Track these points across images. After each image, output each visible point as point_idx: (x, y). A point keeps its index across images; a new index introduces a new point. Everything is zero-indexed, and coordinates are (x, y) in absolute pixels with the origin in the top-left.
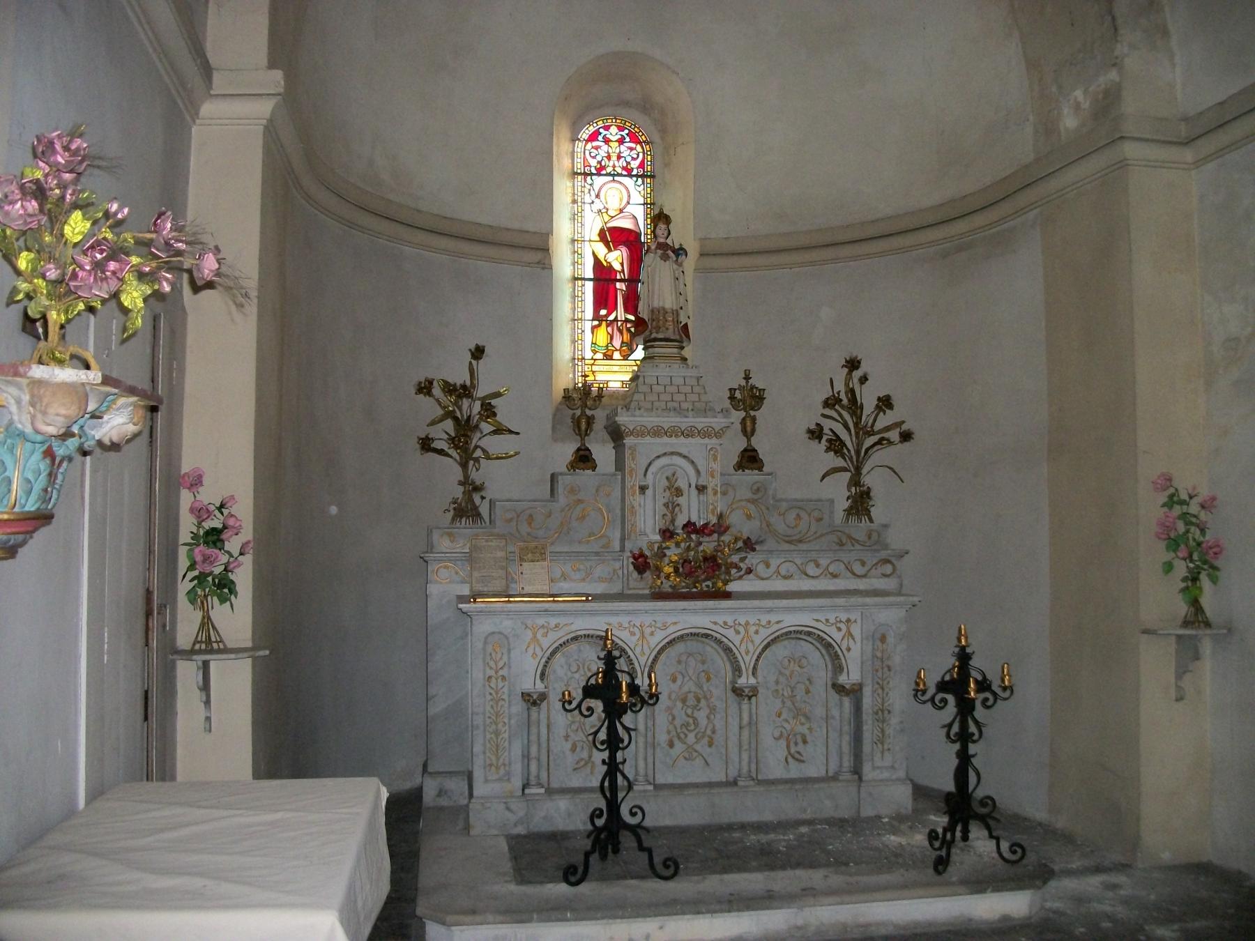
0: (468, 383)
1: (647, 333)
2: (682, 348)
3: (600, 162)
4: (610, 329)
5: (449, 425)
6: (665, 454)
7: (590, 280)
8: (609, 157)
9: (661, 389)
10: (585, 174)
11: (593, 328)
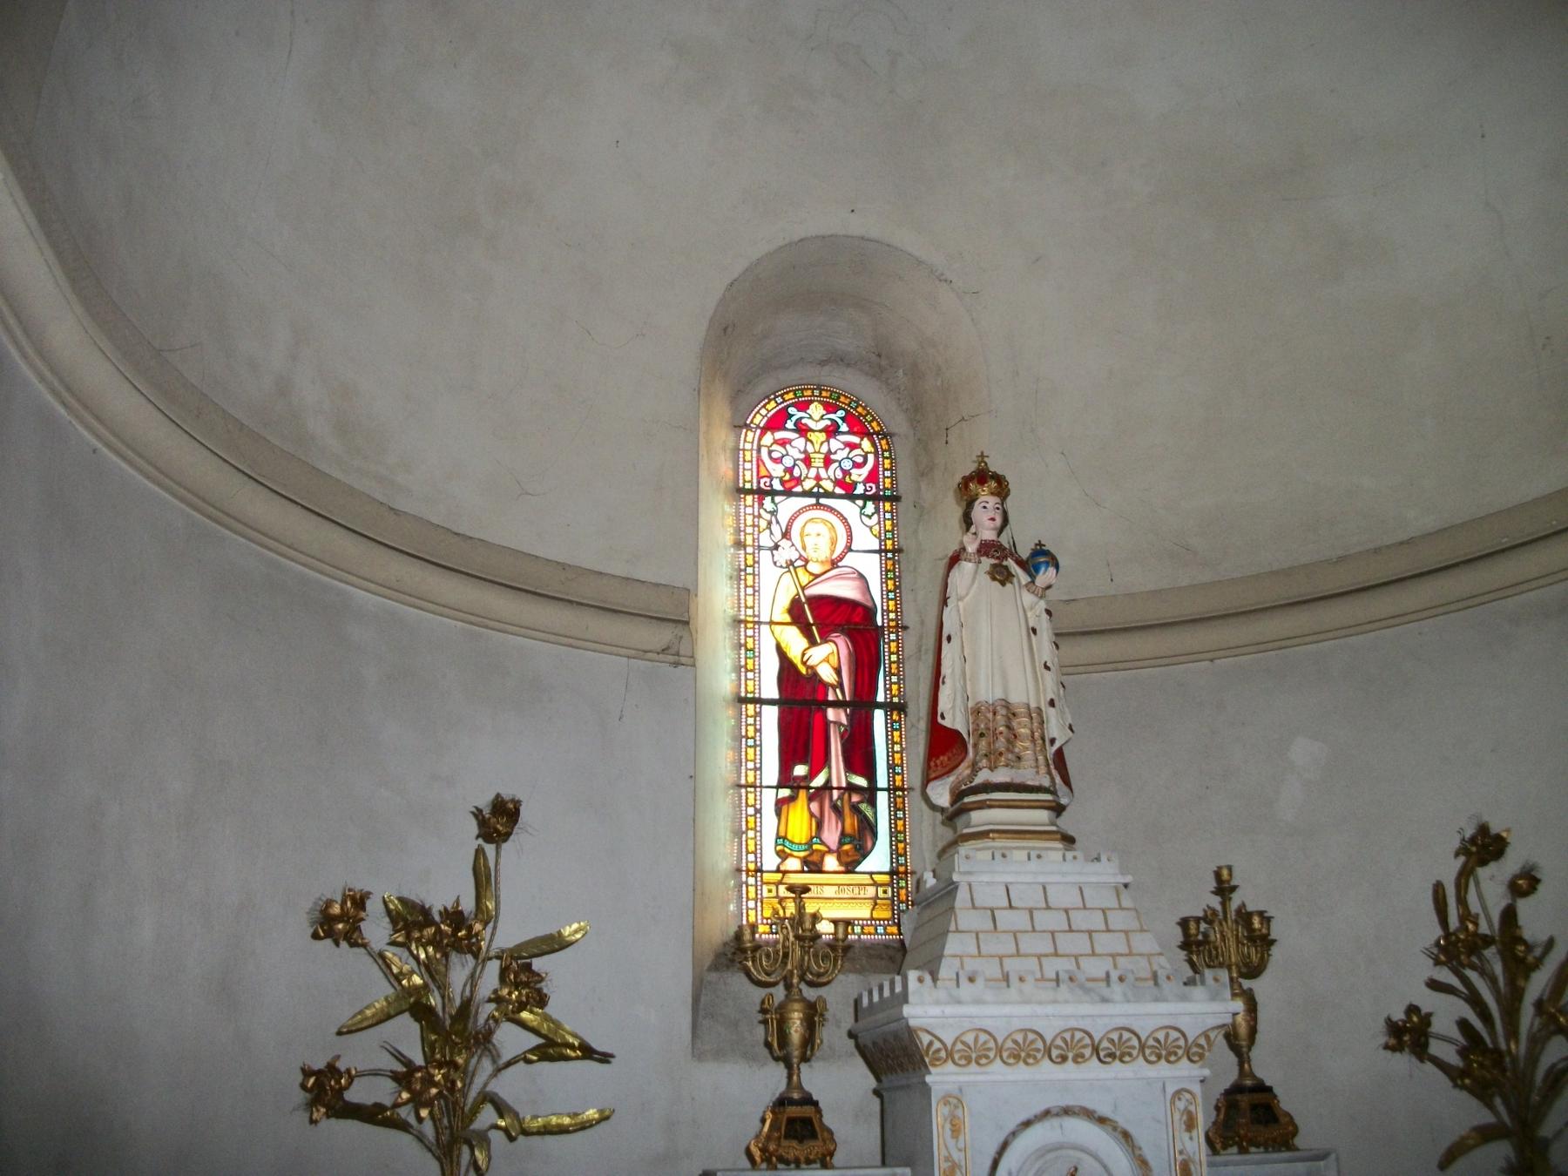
0: (468, 905)
1: (964, 770)
2: (1058, 809)
3: (789, 470)
4: (815, 806)
5: (407, 1036)
6: (1047, 1114)
7: (771, 702)
8: (807, 461)
9: (1019, 920)
10: (761, 493)
11: (780, 804)
